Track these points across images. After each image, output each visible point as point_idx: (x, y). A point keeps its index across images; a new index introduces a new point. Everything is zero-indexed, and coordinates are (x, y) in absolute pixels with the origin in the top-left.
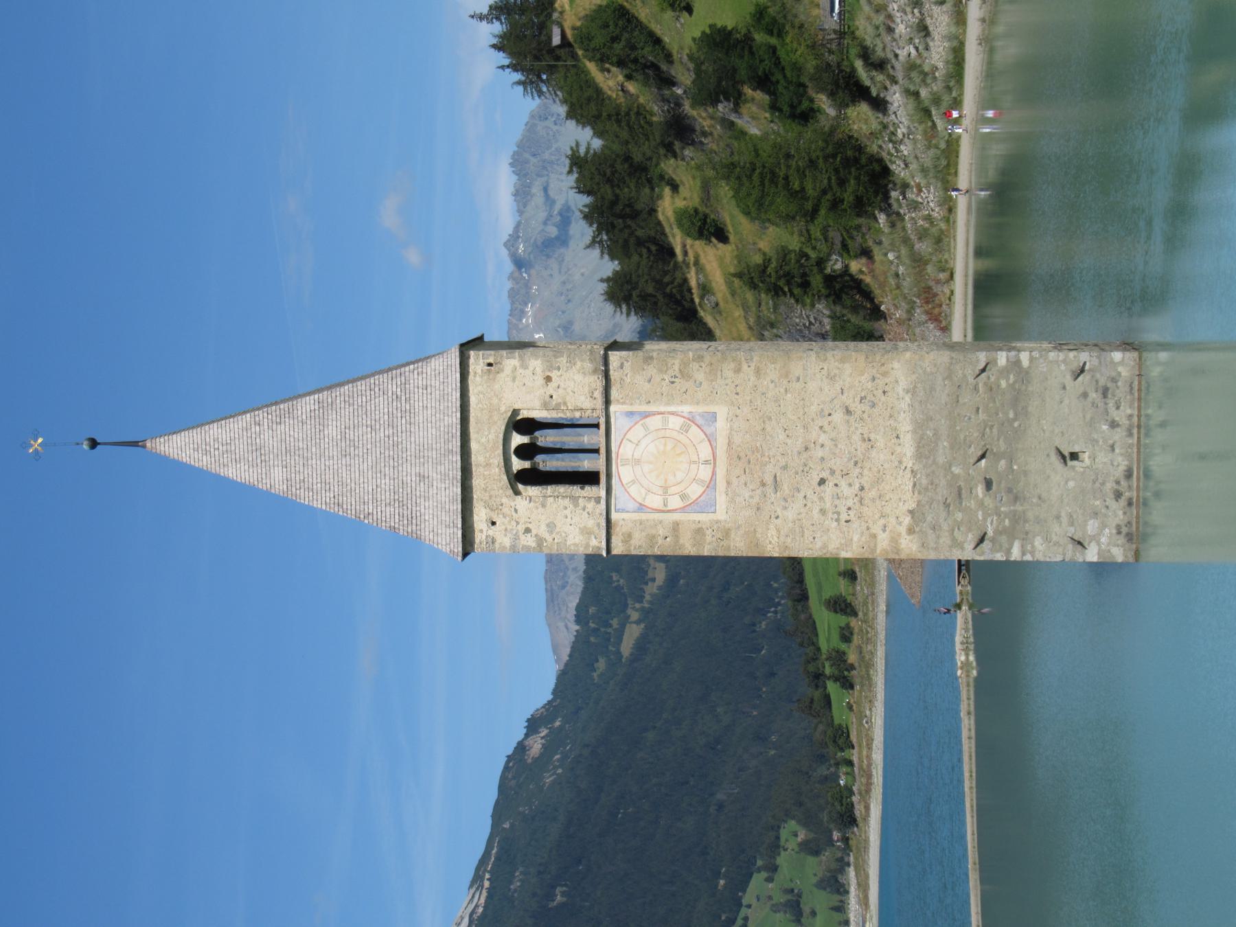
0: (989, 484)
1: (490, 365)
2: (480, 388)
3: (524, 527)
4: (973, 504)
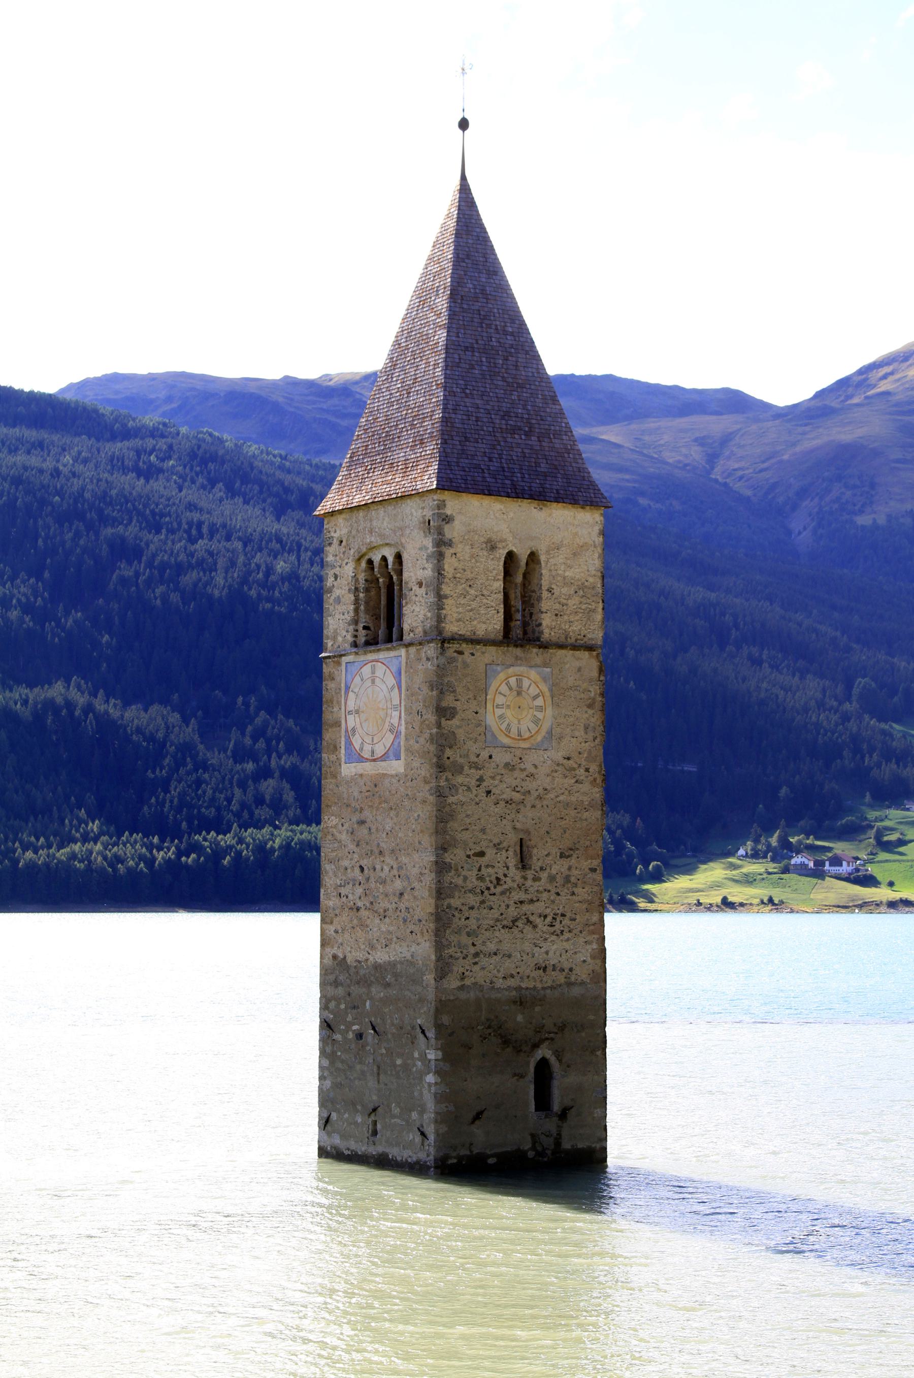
0: (360, 1036)
1: (429, 521)
2: (415, 514)
3: (338, 573)
4: (349, 1018)
